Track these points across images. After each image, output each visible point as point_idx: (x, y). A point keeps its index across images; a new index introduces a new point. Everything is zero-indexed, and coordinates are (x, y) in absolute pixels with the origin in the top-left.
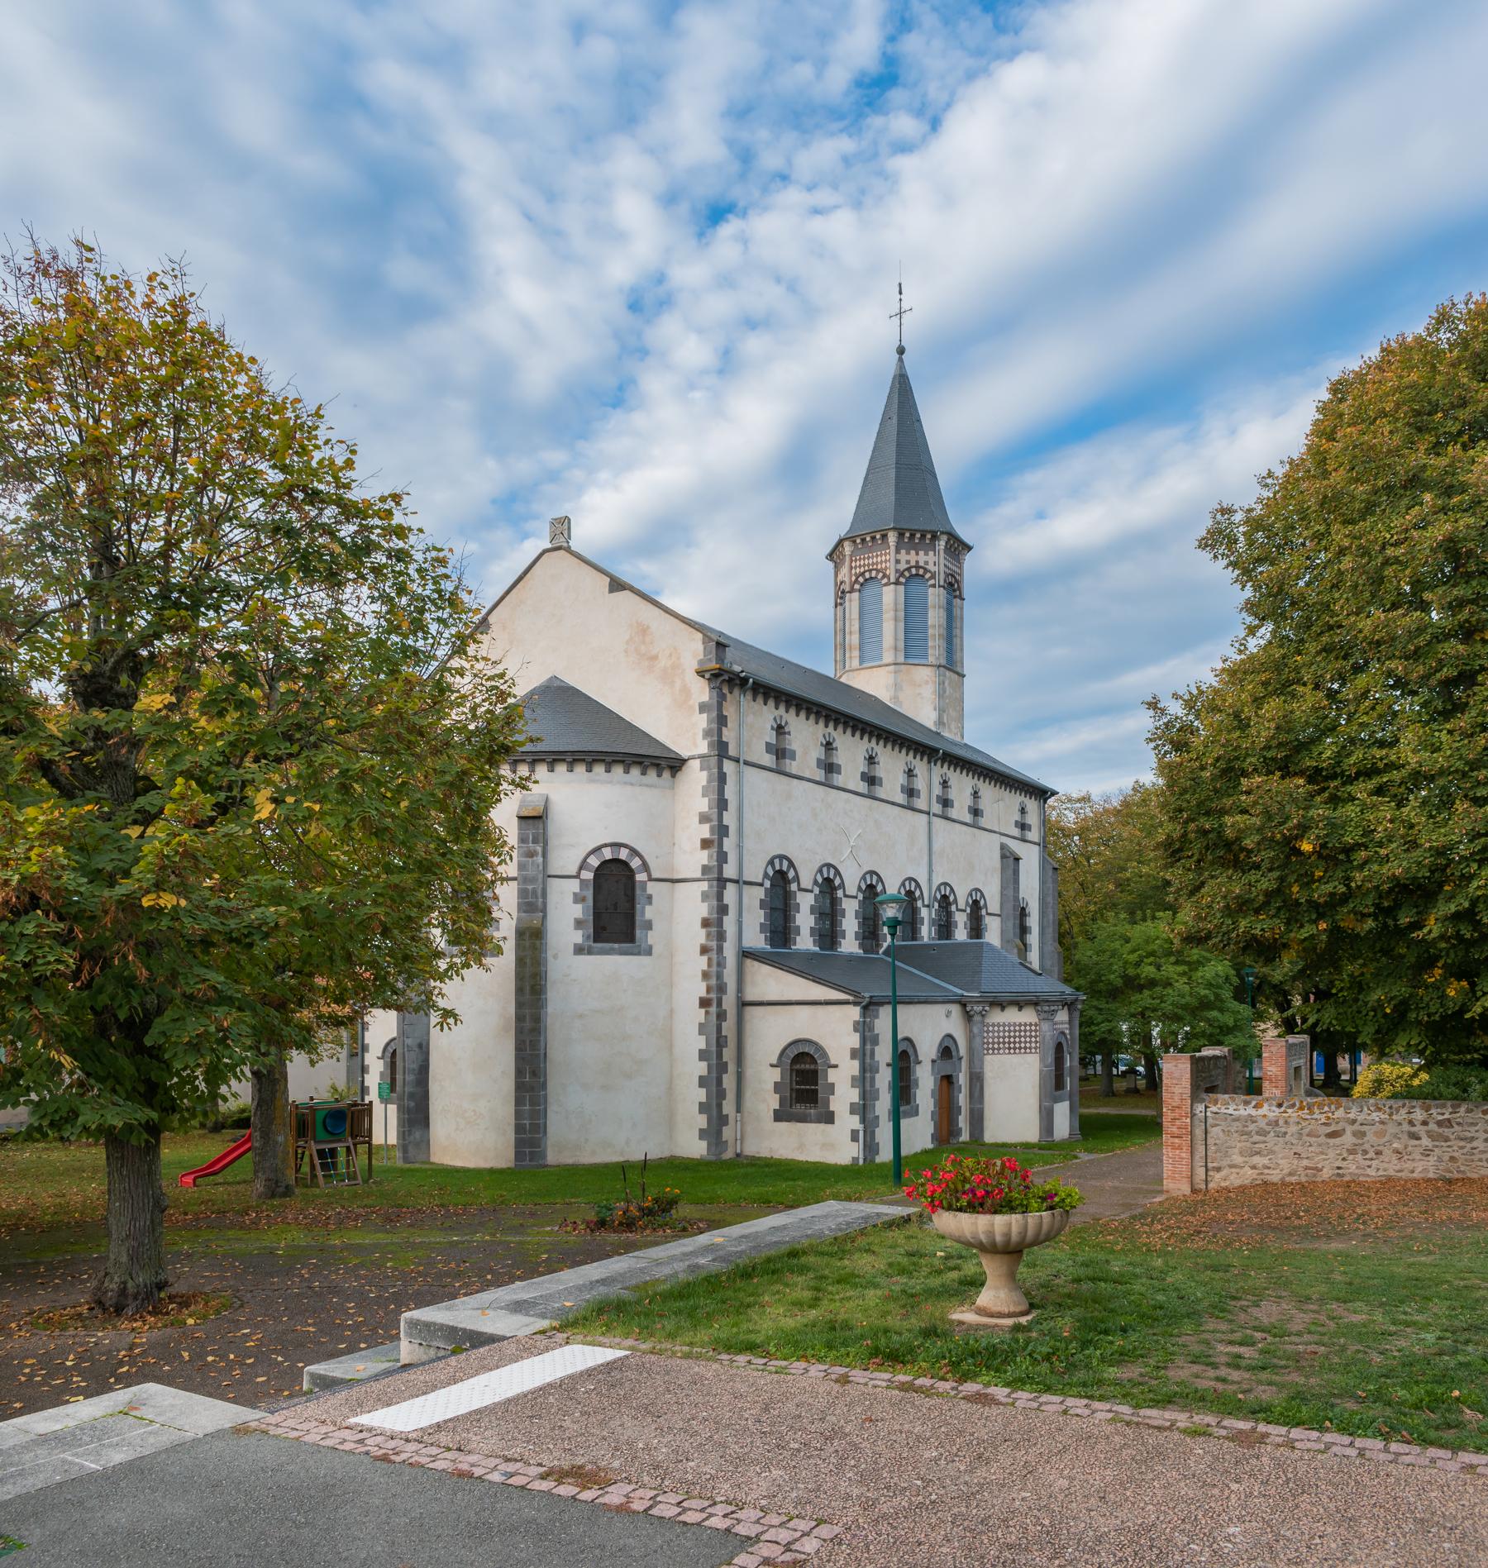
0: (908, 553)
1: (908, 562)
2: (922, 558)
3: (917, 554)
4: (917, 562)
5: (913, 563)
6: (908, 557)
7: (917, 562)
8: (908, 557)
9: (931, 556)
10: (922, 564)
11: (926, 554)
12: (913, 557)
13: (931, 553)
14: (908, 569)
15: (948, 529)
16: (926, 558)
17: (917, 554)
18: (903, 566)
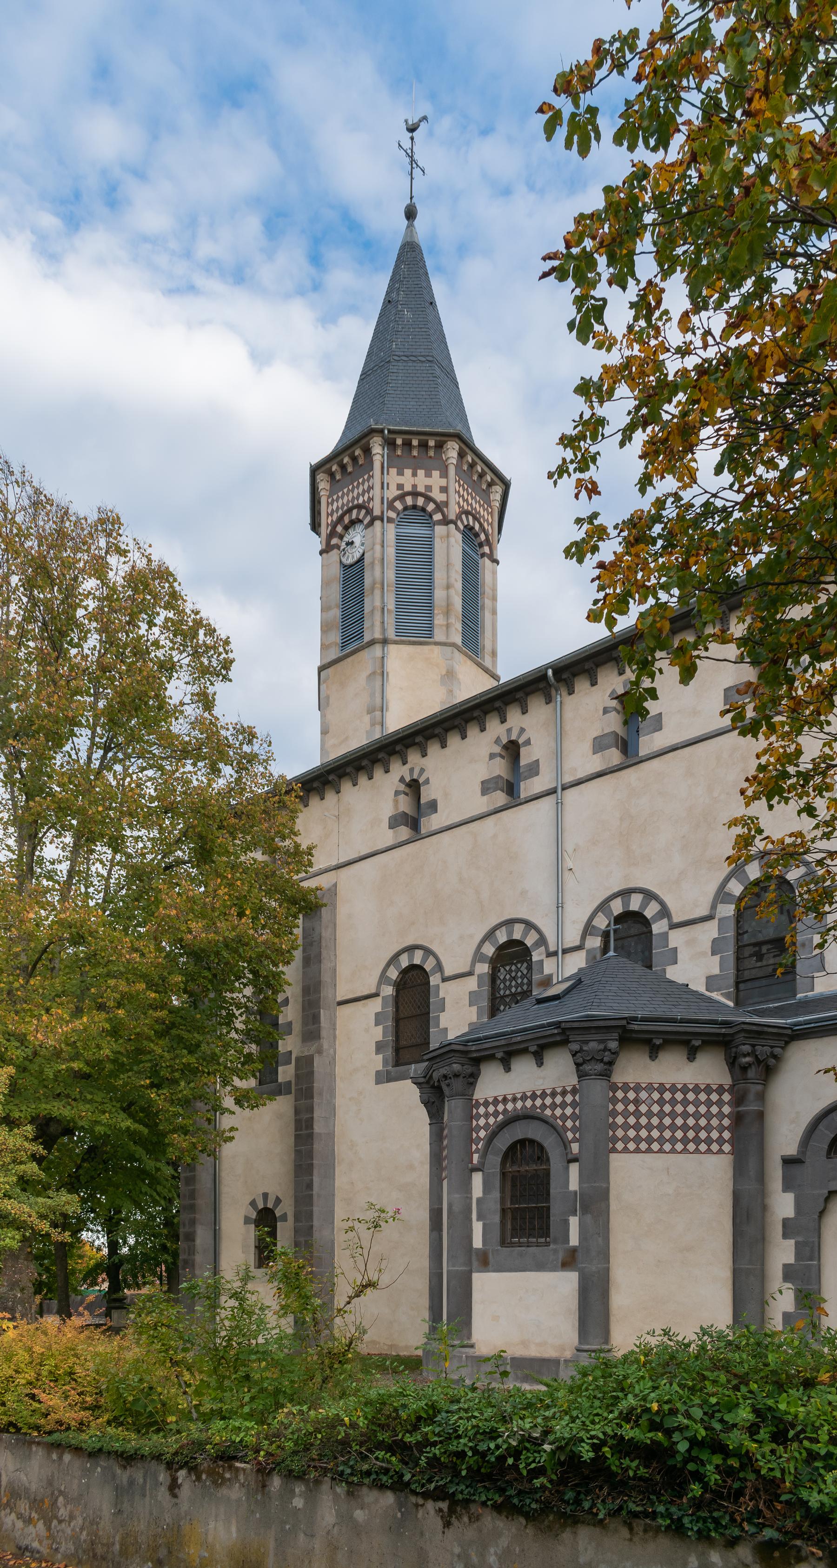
0: (400, 473)
1: (400, 487)
2: (421, 481)
3: (414, 475)
4: (414, 486)
5: (408, 488)
6: (400, 480)
7: (414, 486)
8: (400, 480)
9: (436, 480)
10: (421, 489)
11: (428, 475)
12: (408, 480)
13: (436, 474)
14: (401, 497)
15: (459, 428)
16: (428, 481)
17: (414, 475)
18: (393, 492)
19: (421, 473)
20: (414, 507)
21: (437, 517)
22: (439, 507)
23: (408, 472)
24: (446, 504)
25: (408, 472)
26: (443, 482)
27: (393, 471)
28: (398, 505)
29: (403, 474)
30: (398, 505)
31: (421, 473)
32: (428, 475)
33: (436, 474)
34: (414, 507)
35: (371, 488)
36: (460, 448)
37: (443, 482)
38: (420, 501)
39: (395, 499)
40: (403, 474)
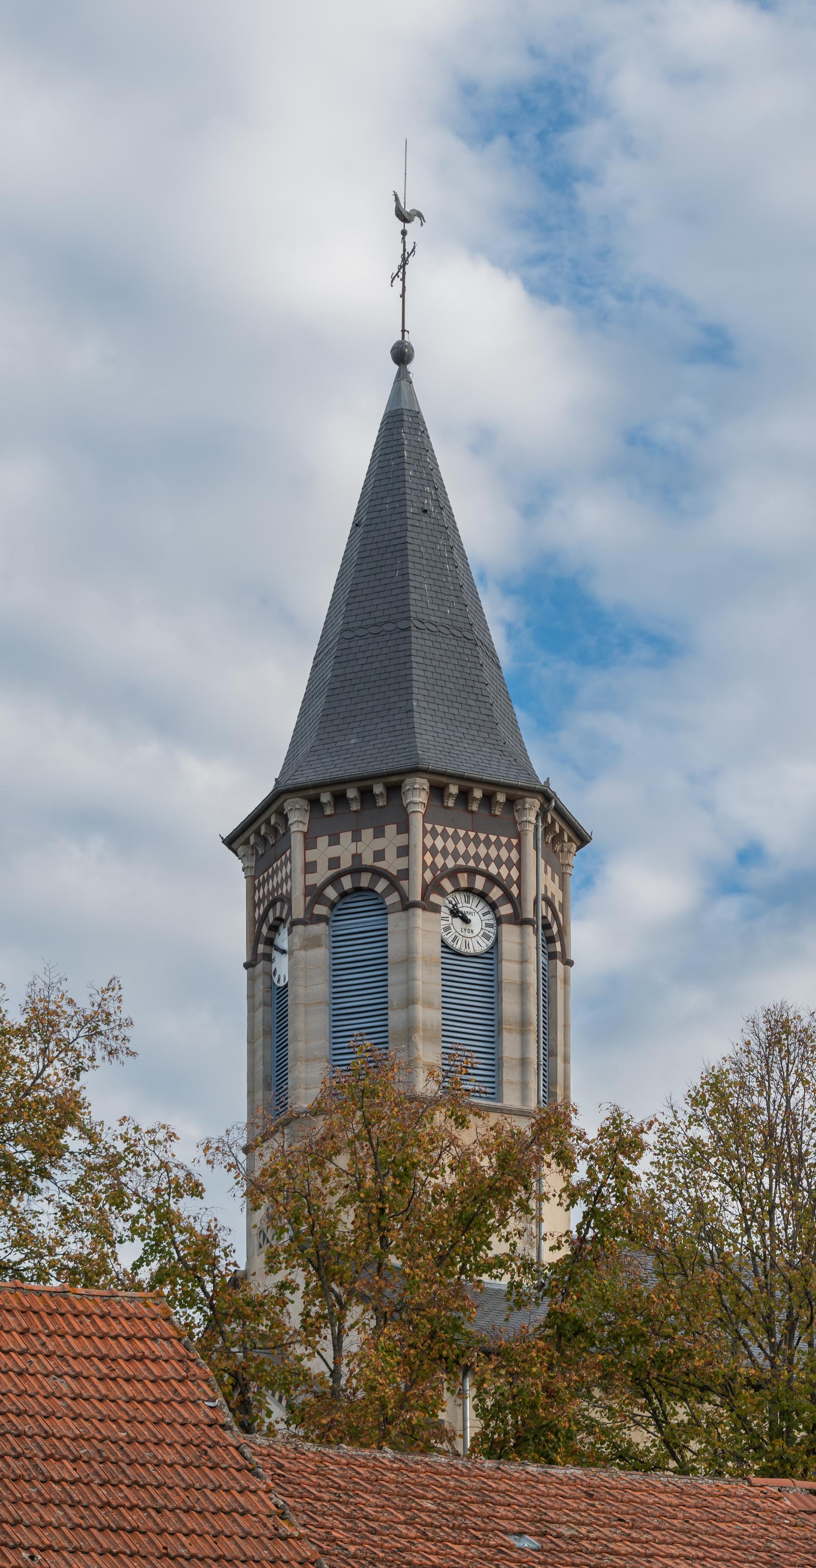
0: (334, 841)
3: (356, 838)
4: (357, 857)
6: (334, 851)
7: (357, 857)
8: (334, 851)
11: (379, 833)
13: (391, 830)
14: (334, 880)
16: (379, 844)
17: (356, 838)
19: (367, 834)
20: (357, 890)
21: (392, 899)
22: (394, 883)
23: (346, 837)
24: (405, 874)
25: (346, 837)
26: (402, 840)
27: (323, 841)
28: (331, 893)
29: (338, 843)
30: (331, 893)
31: (367, 834)
32: (379, 833)
33: (391, 830)
34: (357, 890)
35: (289, 877)
36: (429, 781)
37: (402, 840)
38: (365, 880)
39: (325, 885)
40: (338, 843)
